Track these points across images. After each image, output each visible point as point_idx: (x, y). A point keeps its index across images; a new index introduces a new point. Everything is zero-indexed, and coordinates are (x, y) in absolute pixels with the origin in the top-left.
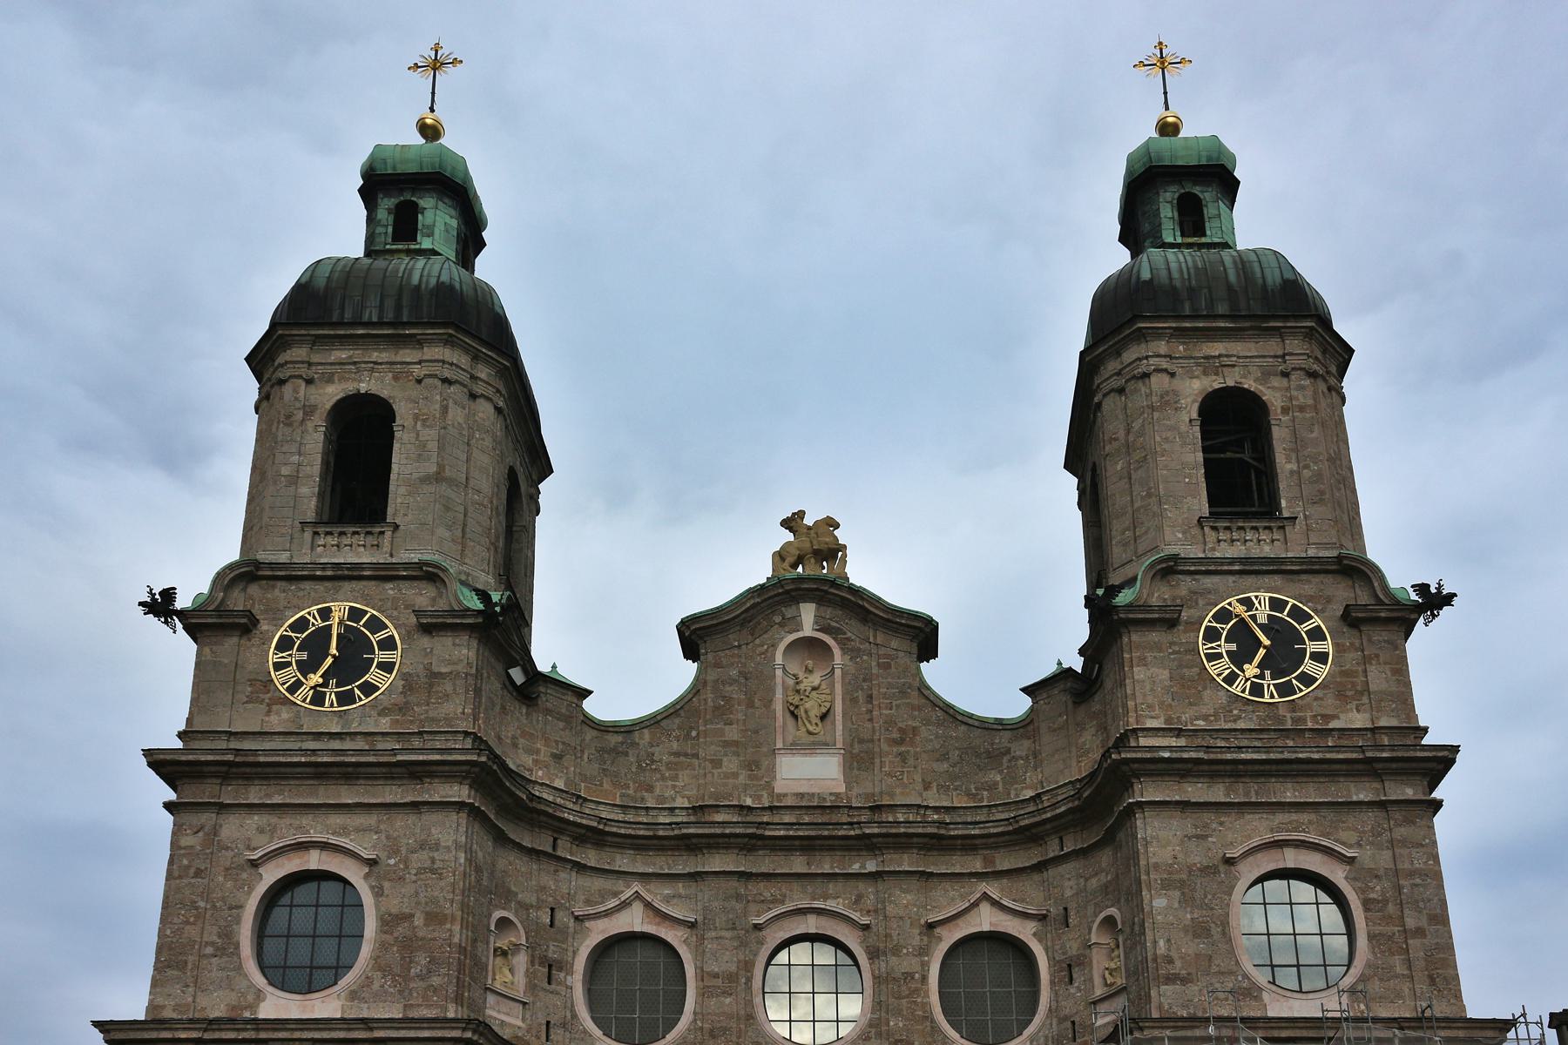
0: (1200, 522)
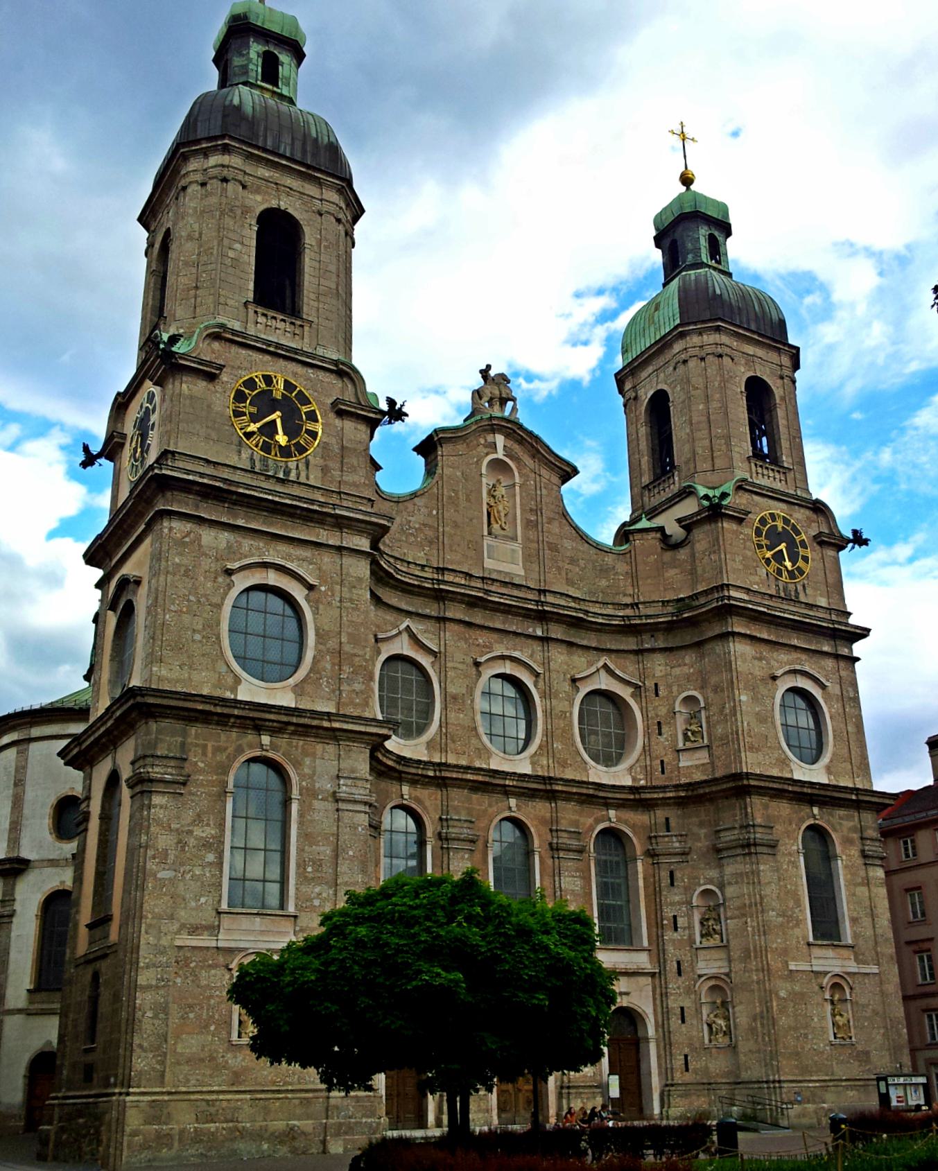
0: (748, 458)
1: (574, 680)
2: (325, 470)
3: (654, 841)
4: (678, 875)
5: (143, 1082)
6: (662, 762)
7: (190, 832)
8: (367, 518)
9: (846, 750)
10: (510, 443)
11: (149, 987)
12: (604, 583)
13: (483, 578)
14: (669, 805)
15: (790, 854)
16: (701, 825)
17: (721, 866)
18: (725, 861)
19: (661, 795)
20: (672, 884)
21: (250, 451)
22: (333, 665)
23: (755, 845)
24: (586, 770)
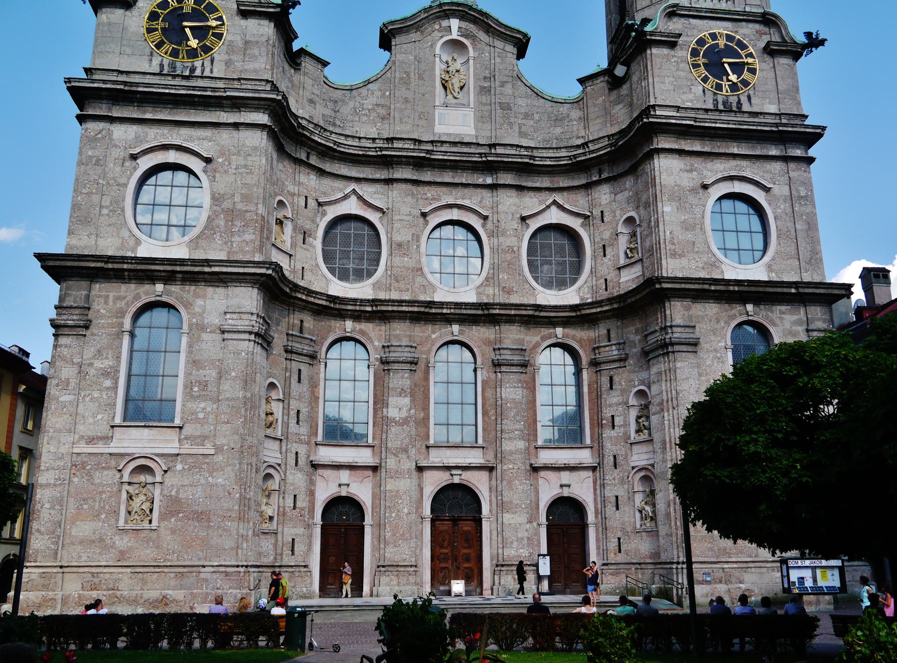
1: (523, 219)
2: (228, 63)
3: (597, 351)
4: (616, 379)
5: (39, 559)
6: (606, 280)
7: (91, 364)
8: (257, 95)
9: (793, 246)
10: (464, 25)
11: (48, 485)
12: (558, 130)
13: (432, 142)
14: (608, 318)
15: (716, 351)
16: (637, 332)
17: (648, 368)
18: (651, 362)
19: (599, 310)
20: (611, 388)
21: (160, 58)
22: (227, 221)
23: (672, 344)
24: (535, 296)
